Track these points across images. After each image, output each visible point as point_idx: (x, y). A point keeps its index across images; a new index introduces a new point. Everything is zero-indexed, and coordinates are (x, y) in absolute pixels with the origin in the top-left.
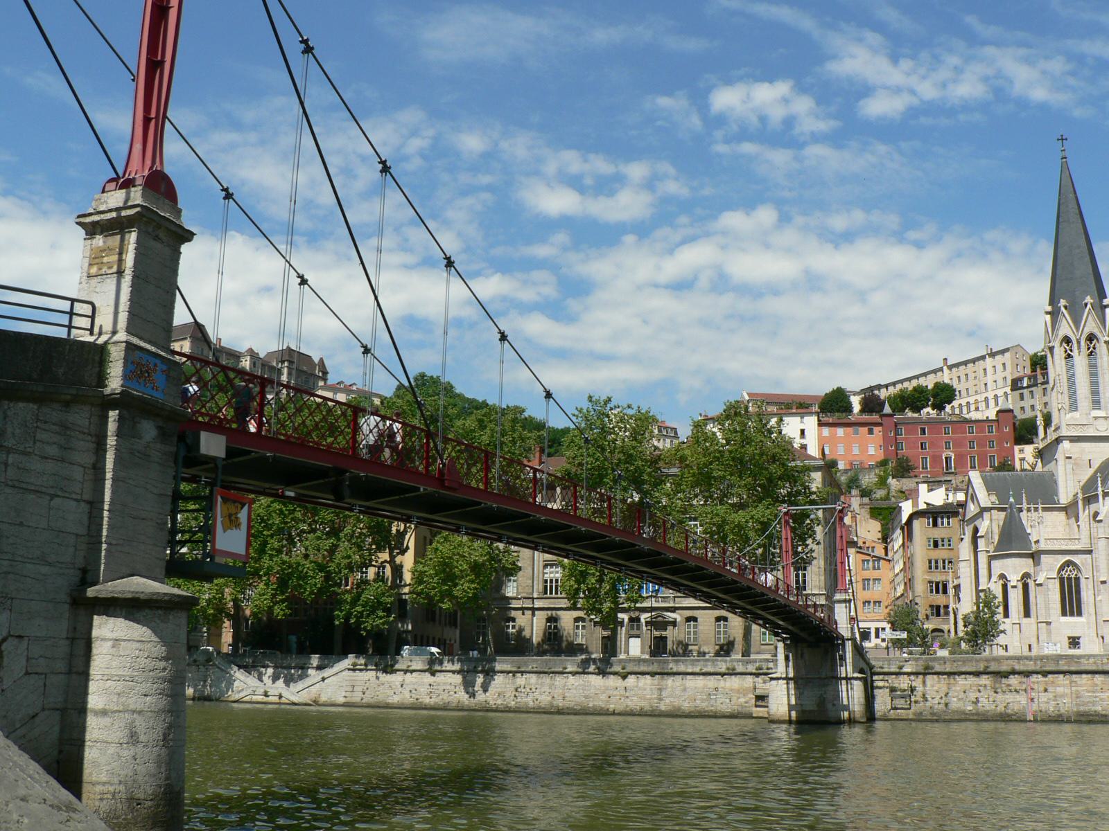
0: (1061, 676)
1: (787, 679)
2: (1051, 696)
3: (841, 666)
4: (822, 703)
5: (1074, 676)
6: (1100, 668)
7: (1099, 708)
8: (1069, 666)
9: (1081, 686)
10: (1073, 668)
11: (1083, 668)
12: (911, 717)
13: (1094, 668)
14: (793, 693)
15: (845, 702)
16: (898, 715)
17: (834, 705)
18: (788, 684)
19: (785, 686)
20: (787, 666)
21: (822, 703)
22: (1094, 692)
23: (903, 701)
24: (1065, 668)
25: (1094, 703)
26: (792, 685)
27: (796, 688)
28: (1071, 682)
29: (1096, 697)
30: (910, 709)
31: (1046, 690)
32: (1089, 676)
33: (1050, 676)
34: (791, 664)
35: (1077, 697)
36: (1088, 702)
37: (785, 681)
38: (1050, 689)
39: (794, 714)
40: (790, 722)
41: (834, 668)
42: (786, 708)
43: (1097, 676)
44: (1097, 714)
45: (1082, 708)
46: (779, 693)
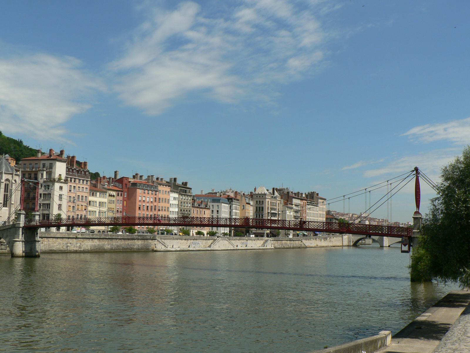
0: (46, 238)
1: (23, 241)
2: (43, 245)
3: (36, 237)
4: (31, 249)
5: (49, 239)
6: (55, 236)
7: (54, 248)
8: (48, 235)
9: (50, 242)
10: (49, 236)
11: (51, 236)
12: (7, 252)
13: (53, 236)
14: (24, 246)
15: (37, 250)
16: (2, 251)
17: (34, 250)
18: (22, 243)
19: (22, 244)
20: (22, 237)
21: (31, 249)
22: (53, 244)
23: (4, 247)
24: (47, 236)
25: (53, 247)
26: (24, 244)
27: (25, 245)
28: (48, 240)
29: (54, 245)
30: (6, 249)
31: (42, 243)
32: (52, 239)
33: (43, 238)
34: (23, 236)
35: (50, 245)
36: (52, 247)
37: (22, 242)
38: (43, 243)
39: (24, 254)
40: (22, 257)
41: (34, 237)
42: (22, 252)
43: (54, 239)
44: (54, 250)
45: (51, 249)
46: (20, 246)
